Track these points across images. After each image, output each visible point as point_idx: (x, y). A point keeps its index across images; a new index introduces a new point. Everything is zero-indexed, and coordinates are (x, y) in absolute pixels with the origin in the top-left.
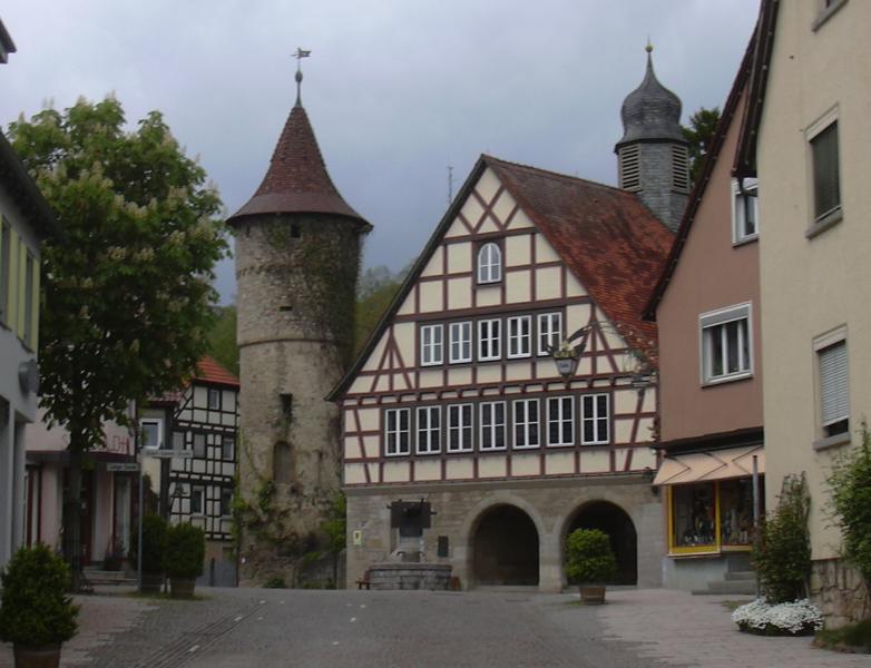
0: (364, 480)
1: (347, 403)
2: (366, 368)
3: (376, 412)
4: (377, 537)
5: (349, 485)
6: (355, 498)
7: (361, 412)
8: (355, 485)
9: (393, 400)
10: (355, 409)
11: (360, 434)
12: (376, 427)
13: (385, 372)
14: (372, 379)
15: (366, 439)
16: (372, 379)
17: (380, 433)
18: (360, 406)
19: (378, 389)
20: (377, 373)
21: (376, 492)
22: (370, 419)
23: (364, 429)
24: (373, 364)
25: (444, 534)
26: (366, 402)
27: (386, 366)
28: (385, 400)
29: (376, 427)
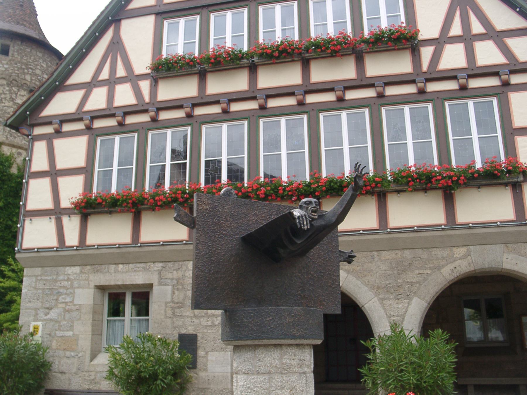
0: (53, 242)
1: (38, 131)
2: (73, 80)
3: (83, 141)
4: (70, 333)
5: (29, 250)
6: (38, 271)
7: (58, 143)
8: (39, 250)
9: (111, 122)
10: (49, 139)
11: (54, 174)
12: (81, 162)
13: (103, 83)
14: (79, 94)
15: (62, 181)
16: (79, 94)
17: (87, 171)
18: (59, 133)
19: (89, 106)
20: (88, 87)
21: (70, 262)
22: (72, 151)
23: (60, 165)
24: (83, 73)
25: (190, 330)
26: (66, 128)
27: (105, 75)
28: (98, 124)
29: (81, 162)
